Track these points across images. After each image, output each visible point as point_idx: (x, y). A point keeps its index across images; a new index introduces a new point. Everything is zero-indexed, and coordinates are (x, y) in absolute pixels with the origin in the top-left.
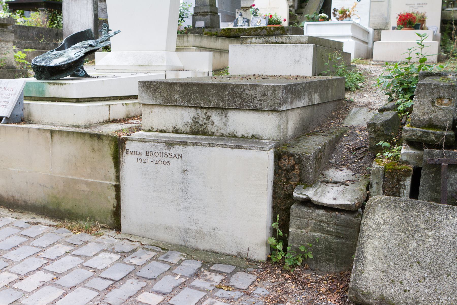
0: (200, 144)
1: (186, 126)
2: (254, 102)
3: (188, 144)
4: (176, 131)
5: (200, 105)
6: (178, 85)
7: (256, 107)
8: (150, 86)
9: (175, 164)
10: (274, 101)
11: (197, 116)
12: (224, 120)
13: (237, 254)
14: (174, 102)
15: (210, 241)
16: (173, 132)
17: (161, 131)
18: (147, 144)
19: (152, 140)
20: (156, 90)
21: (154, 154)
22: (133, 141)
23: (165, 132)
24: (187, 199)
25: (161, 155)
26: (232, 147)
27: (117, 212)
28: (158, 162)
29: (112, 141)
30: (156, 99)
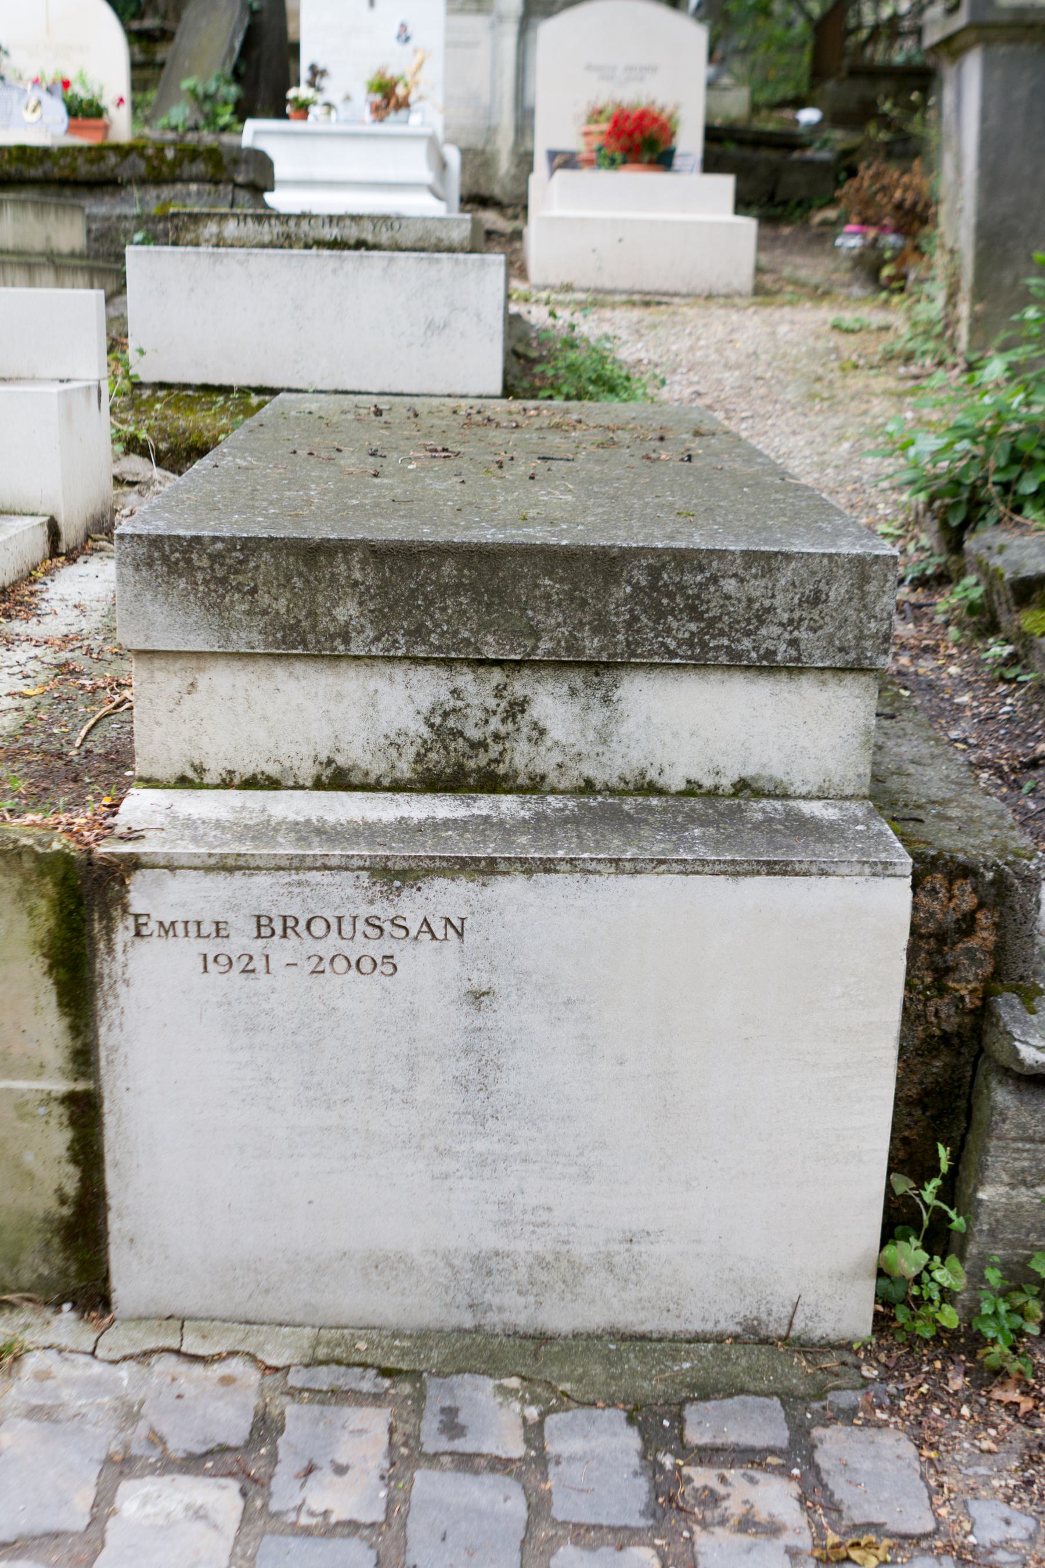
0: (564, 867)
1: (393, 752)
2: (763, 631)
3: (502, 867)
4: (337, 779)
5: (478, 650)
6: (357, 556)
7: (770, 654)
8: (189, 561)
9: (428, 970)
10: (860, 625)
11: (451, 703)
12: (597, 716)
13: (739, 1329)
14: (332, 637)
15: (609, 1291)
16: (318, 785)
17: (251, 783)
18: (262, 880)
19: (292, 858)
20: (223, 581)
21: (301, 928)
22: (172, 868)
23: (273, 784)
24: (491, 1123)
25: (347, 928)
26: (735, 871)
27: (83, 1228)
28: (325, 965)
29: (42, 874)
30: (226, 627)
